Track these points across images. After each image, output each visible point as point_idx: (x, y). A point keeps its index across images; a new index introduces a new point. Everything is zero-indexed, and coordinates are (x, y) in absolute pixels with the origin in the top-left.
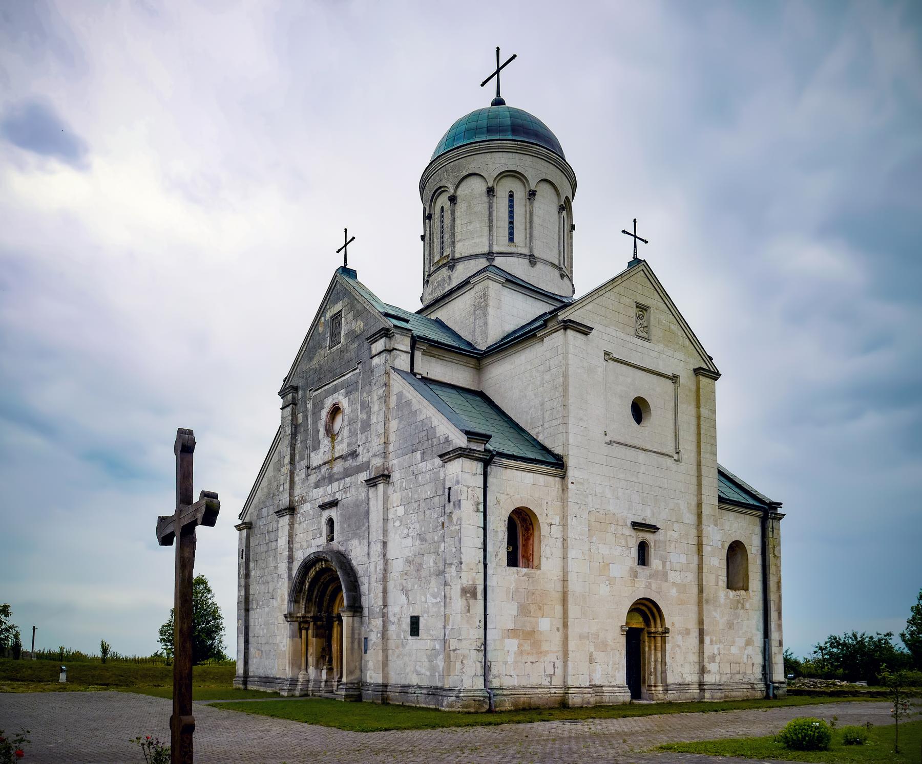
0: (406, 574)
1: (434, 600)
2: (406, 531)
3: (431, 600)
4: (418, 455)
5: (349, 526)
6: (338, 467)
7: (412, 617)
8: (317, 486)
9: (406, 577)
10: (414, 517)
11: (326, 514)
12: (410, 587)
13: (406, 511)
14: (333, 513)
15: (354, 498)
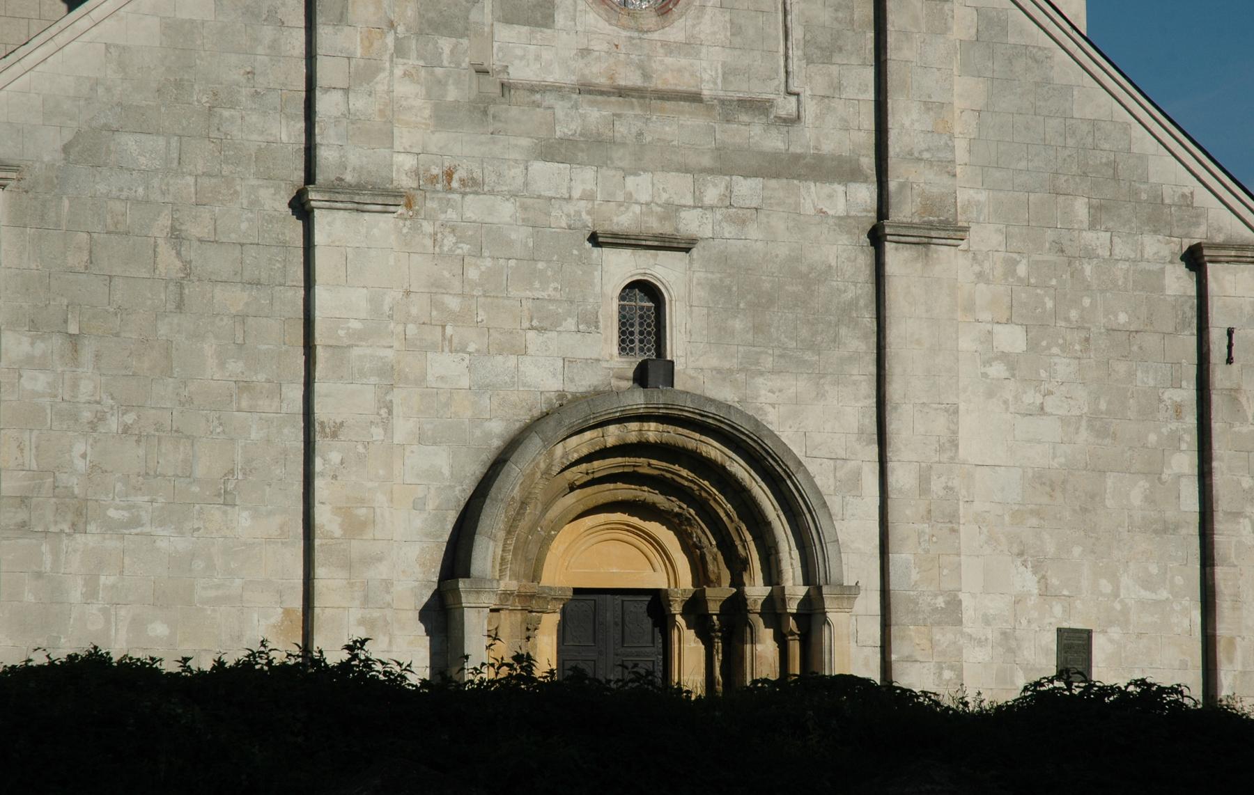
0: (1036, 513)
1: (1146, 594)
2: (1032, 398)
3: (1131, 591)
4: (1081, 208)
5: (757, 329)
6: (680, 127)
7: (1059, 630)
8: (550, 150)
9: (1034, 521)
10: (1064, 367)
11: (622, 267)
12: (1051, 548)
13: (1033, 346)
14: (664, 270)
15: (782, 251)
